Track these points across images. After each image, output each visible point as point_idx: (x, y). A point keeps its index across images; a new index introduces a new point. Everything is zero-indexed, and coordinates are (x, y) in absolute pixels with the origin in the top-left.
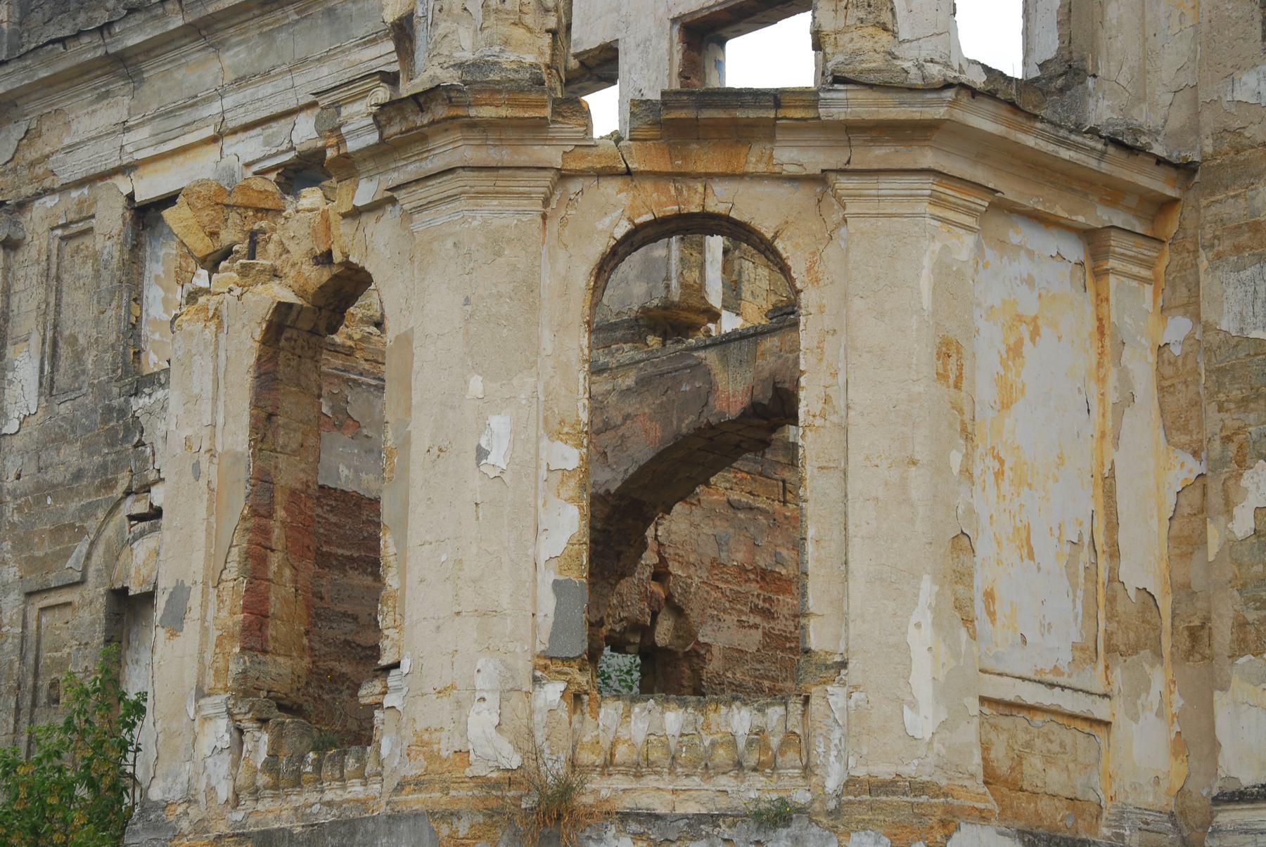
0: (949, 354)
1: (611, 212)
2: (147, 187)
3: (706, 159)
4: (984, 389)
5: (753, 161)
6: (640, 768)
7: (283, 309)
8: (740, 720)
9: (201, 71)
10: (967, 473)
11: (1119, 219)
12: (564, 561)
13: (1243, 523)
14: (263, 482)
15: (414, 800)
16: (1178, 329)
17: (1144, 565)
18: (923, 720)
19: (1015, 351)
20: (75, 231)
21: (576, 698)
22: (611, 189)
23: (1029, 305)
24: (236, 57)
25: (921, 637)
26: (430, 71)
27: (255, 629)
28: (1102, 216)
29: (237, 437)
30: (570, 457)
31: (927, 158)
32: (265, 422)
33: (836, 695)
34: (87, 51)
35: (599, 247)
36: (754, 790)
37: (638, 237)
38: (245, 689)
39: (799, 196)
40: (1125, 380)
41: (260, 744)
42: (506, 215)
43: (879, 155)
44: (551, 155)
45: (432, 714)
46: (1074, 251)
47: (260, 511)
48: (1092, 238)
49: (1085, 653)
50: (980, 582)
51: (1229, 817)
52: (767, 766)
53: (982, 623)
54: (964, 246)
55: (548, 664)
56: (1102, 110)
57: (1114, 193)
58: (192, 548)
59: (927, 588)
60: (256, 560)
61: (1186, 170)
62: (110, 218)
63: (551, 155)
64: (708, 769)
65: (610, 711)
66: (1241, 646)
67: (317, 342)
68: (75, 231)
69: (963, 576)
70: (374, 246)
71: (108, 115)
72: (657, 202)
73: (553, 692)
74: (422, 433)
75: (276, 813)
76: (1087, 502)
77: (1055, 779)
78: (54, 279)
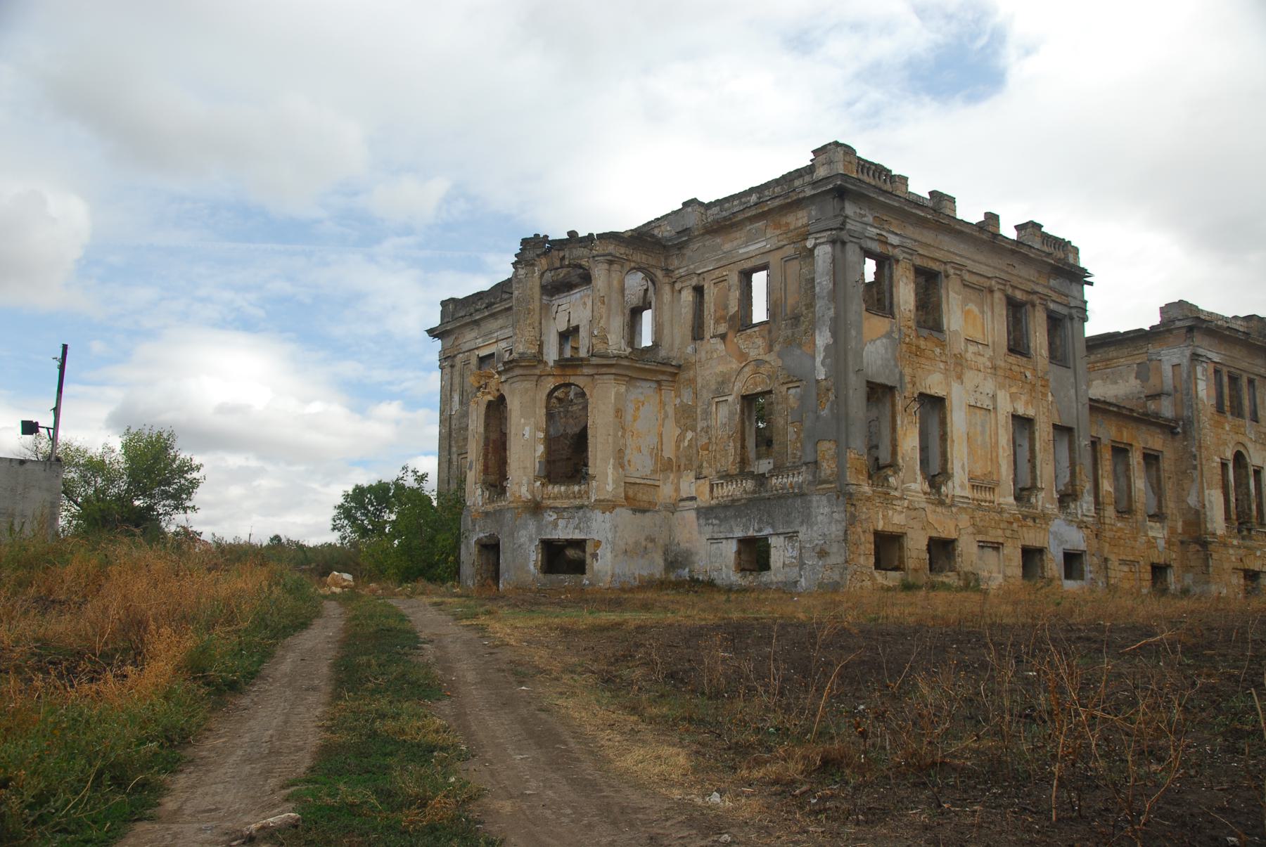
0: (619, 412)
1: (550, 383)
2: (483, 353)
3: (569, 372)
4: (629, 417)
5: (578, 372)
6: (555, 498)
7: (490, 402)
8: (576, 488)
9: (493, 325)
10: (623, 436)
11: (665, 378)
12: (541, 456)
13: (686, 444)
14: (487, 439)
15: (512, 505)
16: (678, 401)
17: (669, 452)
18: (610, 488)
19: (638, 409)
20: (467, 363)
21: (543, 485)
22: (550, 378)
23: (642, 398)
24: (500, 322)
25: (610, 471)
26: (515, 355)
27: (486, 470)
28: (661, 377)
29: (481, 429)
30: (542, 435)
31: (613, 371)
32: (487, 426)
33: (594, 483)
34: (468, 319)
35: (548, 391)
36: (578, 502)
37: (556, 388)
38: (484, 483)
39: (589, 379)
40: (666, 412)
41: (487, 494)
42: (528, 385)
43: (604, 370)
44: (538, 372)
45: (515, 488)
46: (654, 385)
47: (486, 444)
48: (659, 382)
49: (654, 471)
50: (626, 459)
51: (682, 504)
52: (581, 497)
53: (627, 467)
54: (623, 389)
55: (537, 478)
56: (663, 353)
57: (663, 373)
58: (474, 450)
59: (612, 461)
60: (486, 455)
61: (679, 367)
62: (474, 361)
63: (538, 372)
64: (568, 497)
65: (550, 487)
66: (686, 469)
67: (497, 409)
68: (467, 363)
69: (622, 458)
70: (506, 390)
71: (473, 334)
72: (560, 381)
73: (538, 483)
74: (513, 432)
75: (490, 508)
76: (656, 440)
77: (645, 498)
78: (462, 376)
